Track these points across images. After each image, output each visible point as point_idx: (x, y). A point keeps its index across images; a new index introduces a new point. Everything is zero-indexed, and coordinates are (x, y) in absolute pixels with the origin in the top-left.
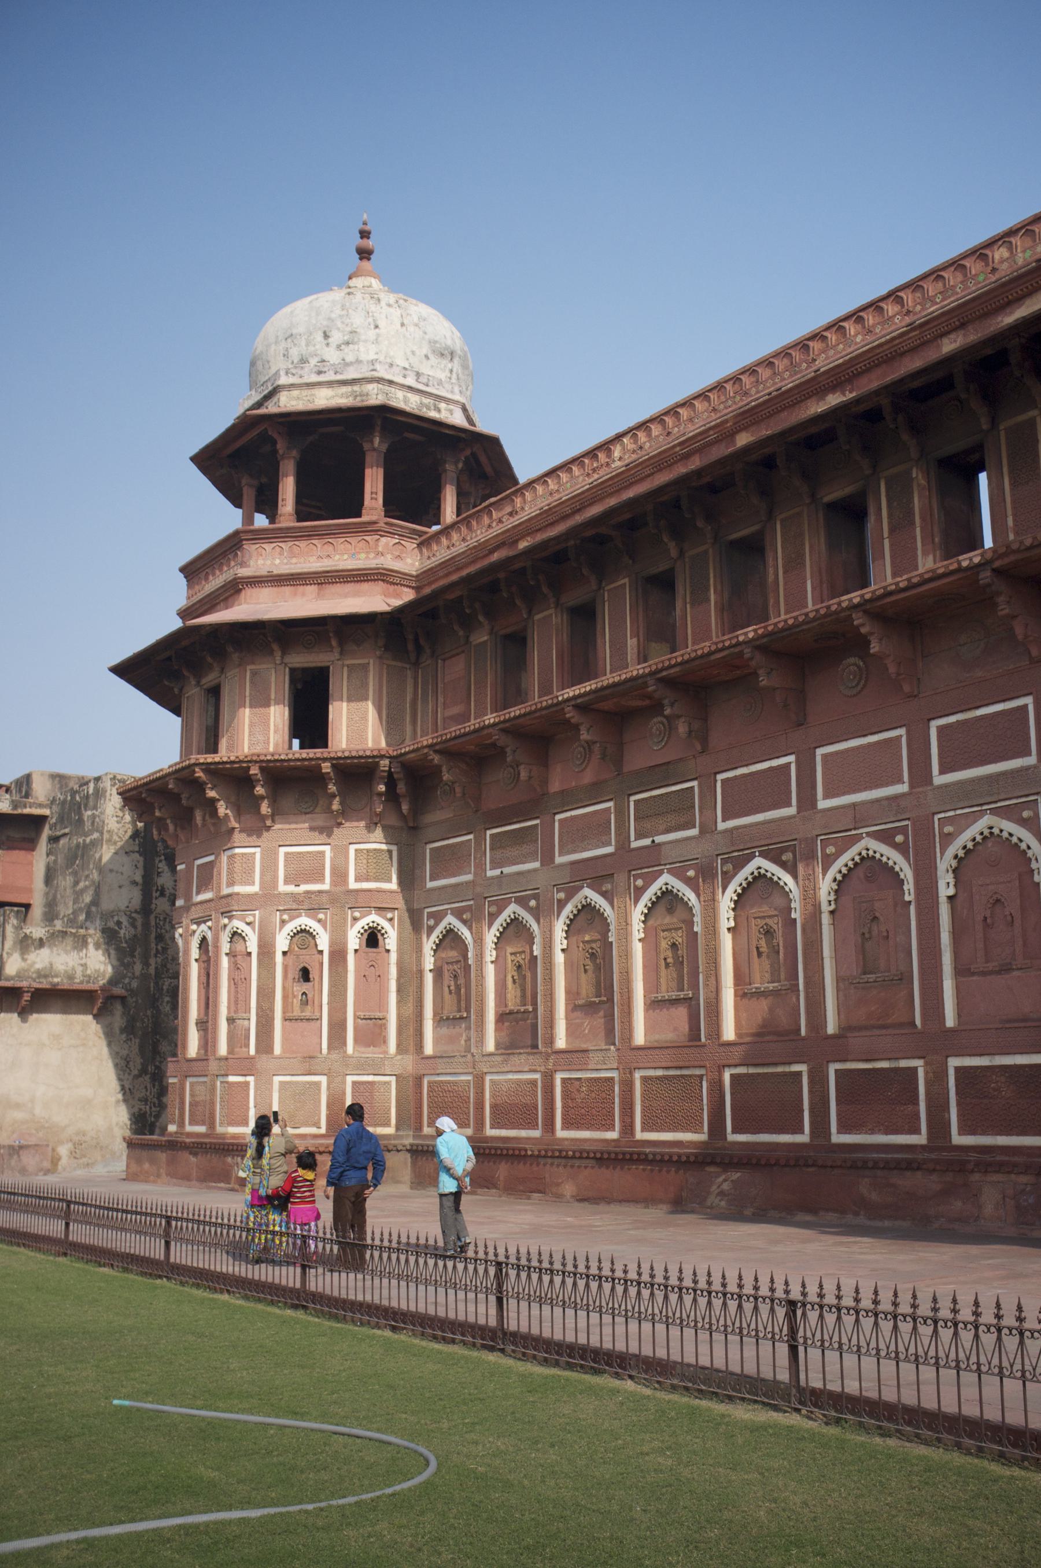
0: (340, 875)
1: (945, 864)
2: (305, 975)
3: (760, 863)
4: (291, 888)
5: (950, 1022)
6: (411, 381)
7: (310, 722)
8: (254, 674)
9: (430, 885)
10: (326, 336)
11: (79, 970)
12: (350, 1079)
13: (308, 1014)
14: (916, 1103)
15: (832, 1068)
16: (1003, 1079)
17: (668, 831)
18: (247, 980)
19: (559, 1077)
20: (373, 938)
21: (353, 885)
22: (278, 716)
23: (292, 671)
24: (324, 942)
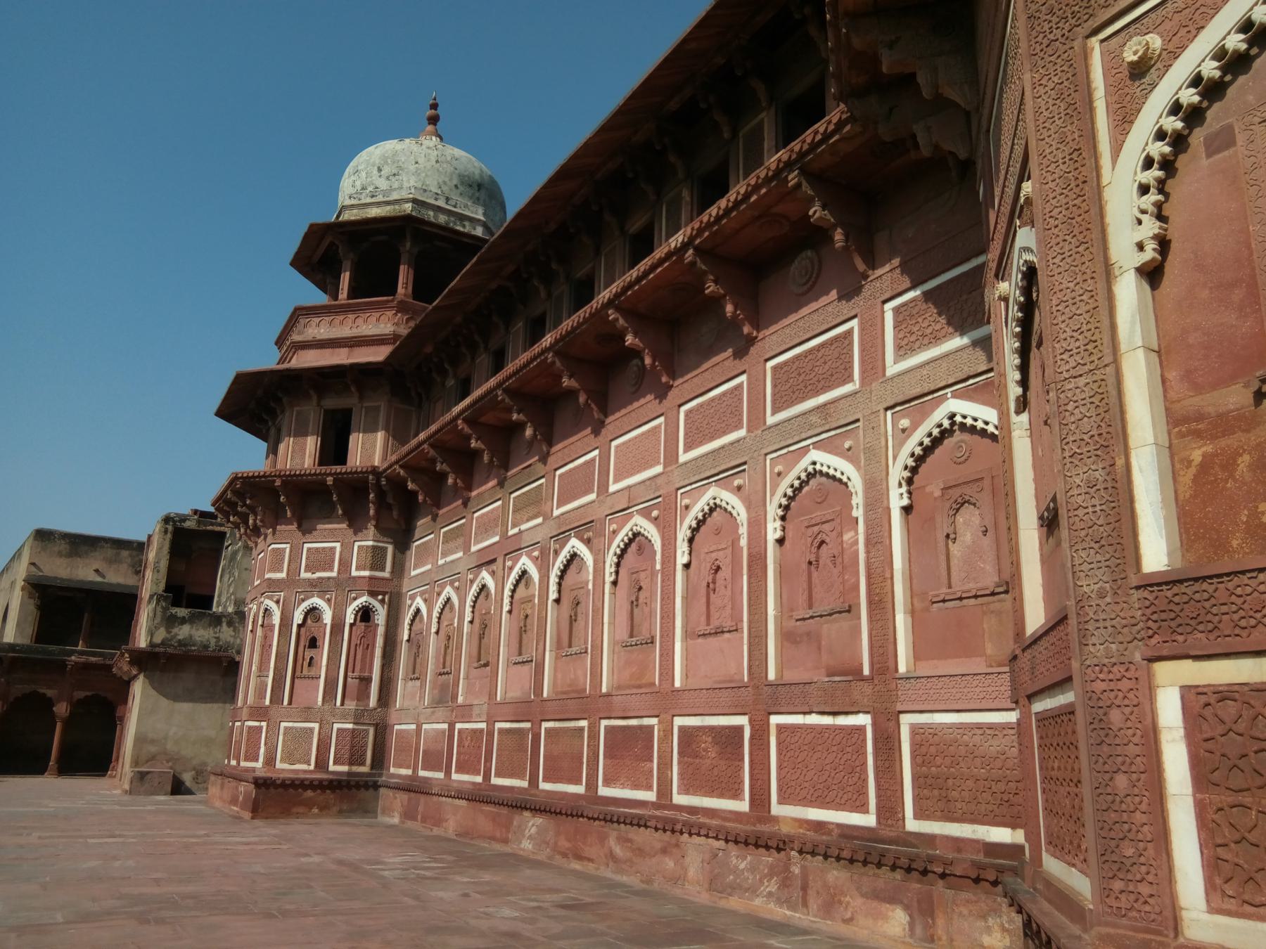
0: (345, 565)
1: (683, 533)
2: (313, 643)
3: (574, 544)
4: (309, 575)
5: (677, 684)
6: (441, 203)
7: (334, 450)
8: (299, 413)
9: (413, 573)
10: (380, 170)
11: (213, 642)
12: (336, 726)
13: (312, 674)
14: (652, 761)
15: (604, 723)
16: (710, 739)
17: (528, 520)
18: (270, 646)
19: (458, 726)
20: (365, 614)
21: (354, 573)
22: (311, 444)
23: (326, 411)
24: (327, 618)
